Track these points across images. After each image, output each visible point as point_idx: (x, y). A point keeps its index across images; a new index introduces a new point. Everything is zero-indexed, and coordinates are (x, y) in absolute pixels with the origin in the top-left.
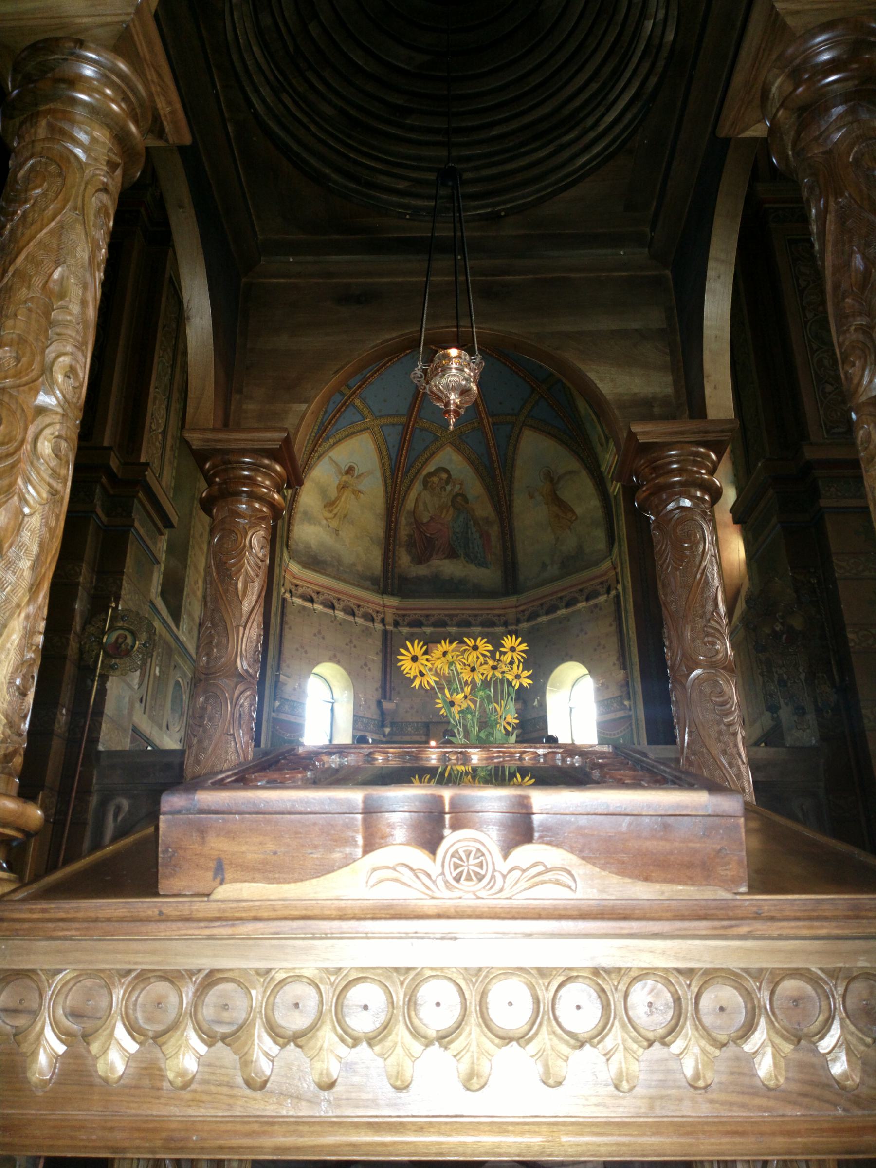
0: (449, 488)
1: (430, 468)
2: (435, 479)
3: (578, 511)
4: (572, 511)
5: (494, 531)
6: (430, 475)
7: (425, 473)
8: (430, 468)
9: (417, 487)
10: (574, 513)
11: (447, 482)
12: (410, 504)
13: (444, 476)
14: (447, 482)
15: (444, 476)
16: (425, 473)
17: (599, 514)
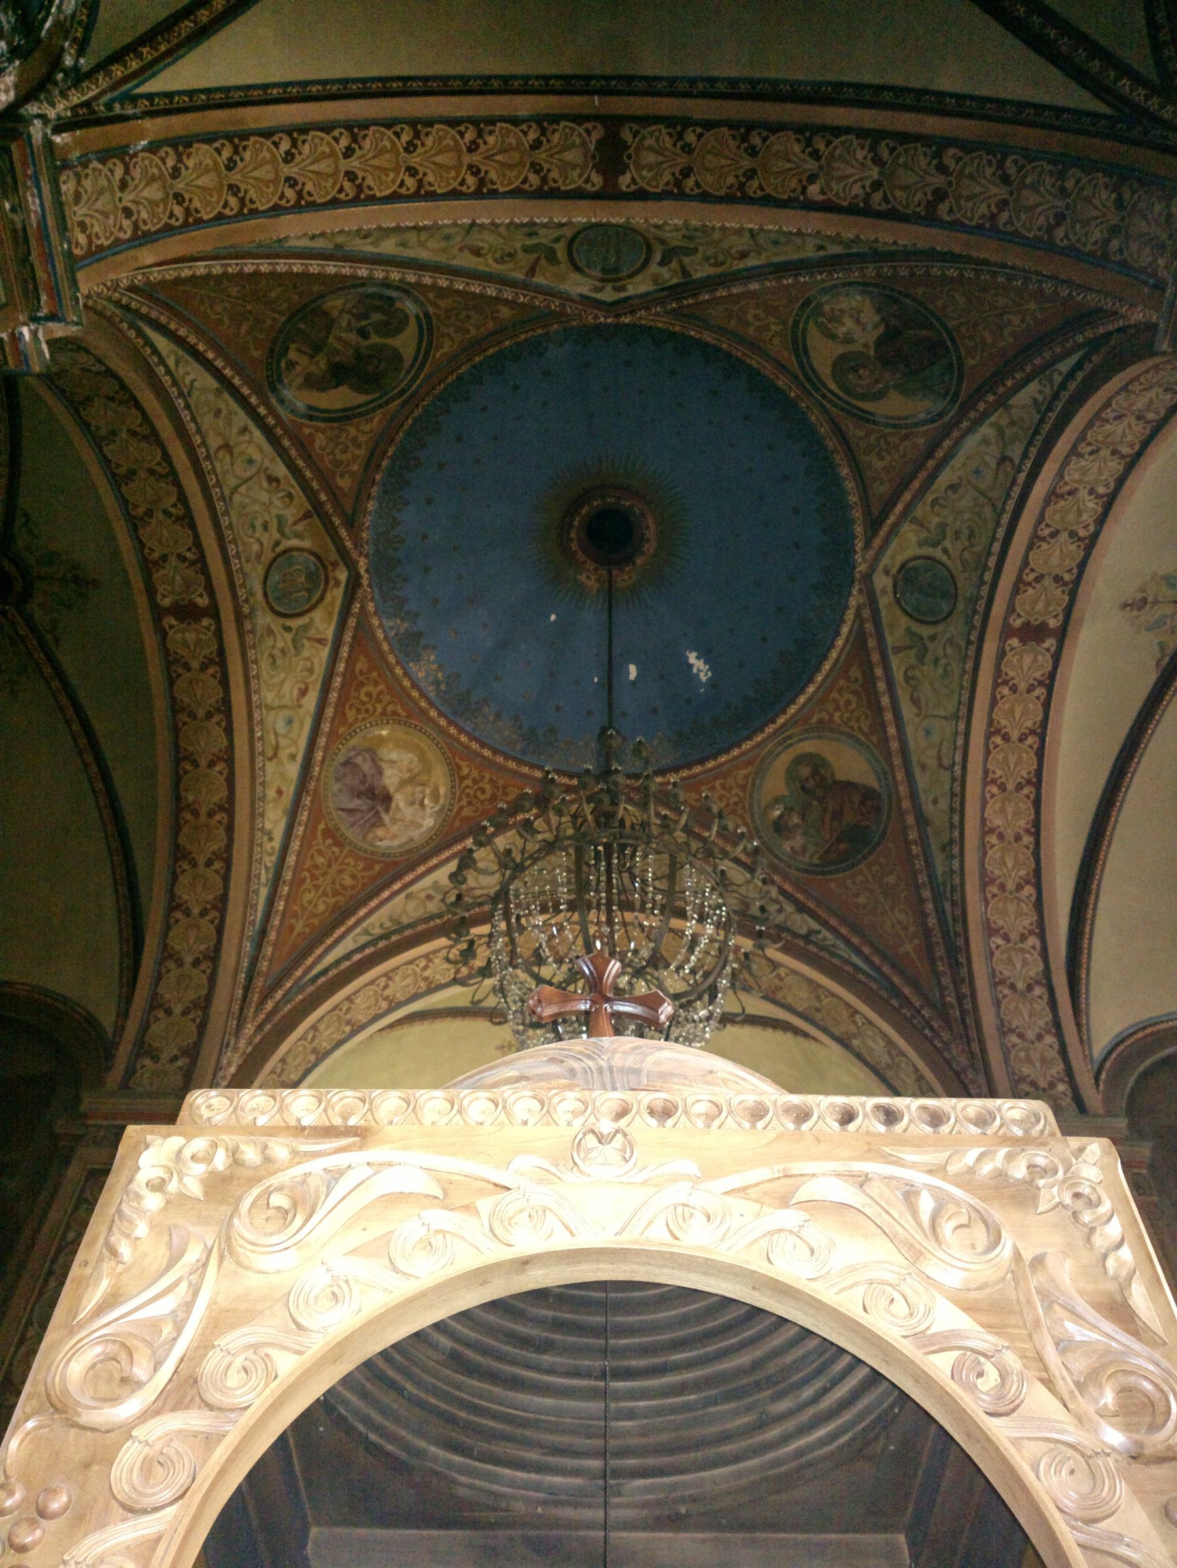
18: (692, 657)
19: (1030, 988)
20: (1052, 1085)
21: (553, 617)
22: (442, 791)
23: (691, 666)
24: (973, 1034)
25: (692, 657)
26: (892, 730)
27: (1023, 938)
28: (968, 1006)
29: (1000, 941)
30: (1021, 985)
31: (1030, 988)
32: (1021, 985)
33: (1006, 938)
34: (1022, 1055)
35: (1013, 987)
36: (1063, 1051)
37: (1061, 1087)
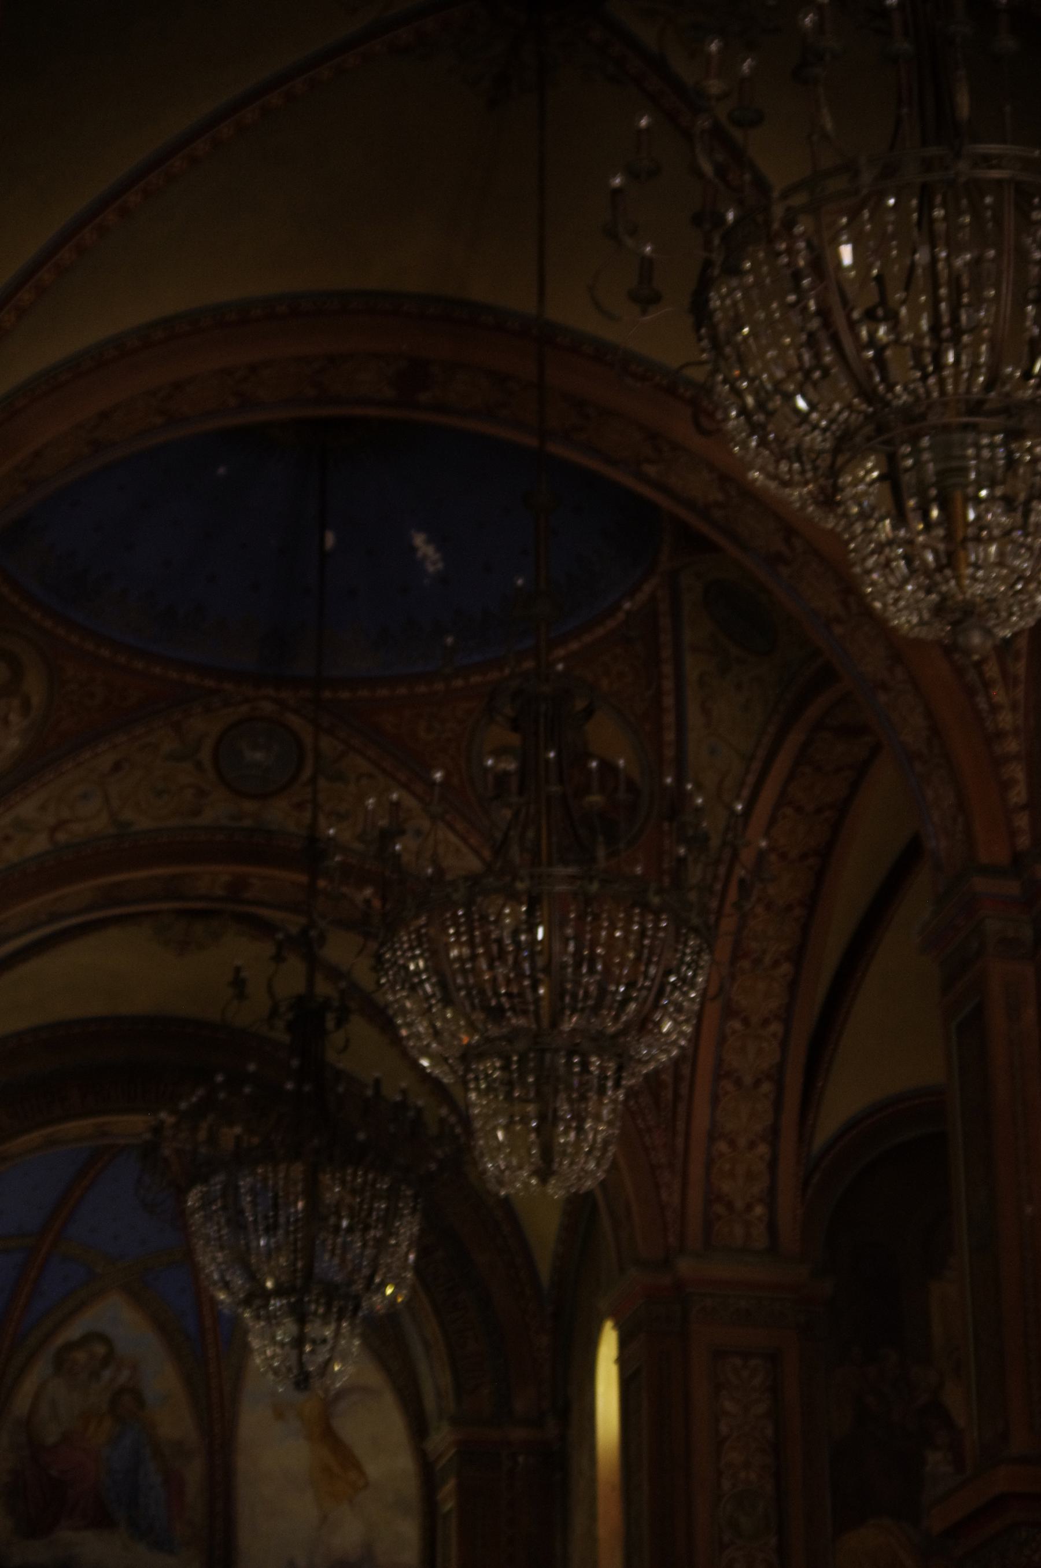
0: (107, 1374)
1: (74, 1331)
2: (81, 1356)
3: (373, 1470)
4: (358, 1467)
5: (194, 1473)
6: (70, 1346)
7: (60, 1340)
8: (74, 1331)
9: (41, 1369)
10: (362, 1473)
11: (107, 1360)
12: (21, 1404)
13: (100, 1350)
14: (107, 1360)
15: (100, 1350)
16: (60, 1340)
17: (411, 1488)
18: (419, 540)
19: (757, 1083)
20: (749, 1207)
21: (222, 471)
22: (35, 700)
23: (413, 549)
24: (681, 1125)
25: (419, 540)
26: (670, 736)
27: (766, 1022)
28: (684, 1090)
29: (737, 1025)
30: (748, 1080)
31: (757, 1083)
32: (748, 1080)
33: (746, 1022)
34: (727, 1167)
35: (738, 1083)
36: (773, 1165)
37: (759, 1210)
